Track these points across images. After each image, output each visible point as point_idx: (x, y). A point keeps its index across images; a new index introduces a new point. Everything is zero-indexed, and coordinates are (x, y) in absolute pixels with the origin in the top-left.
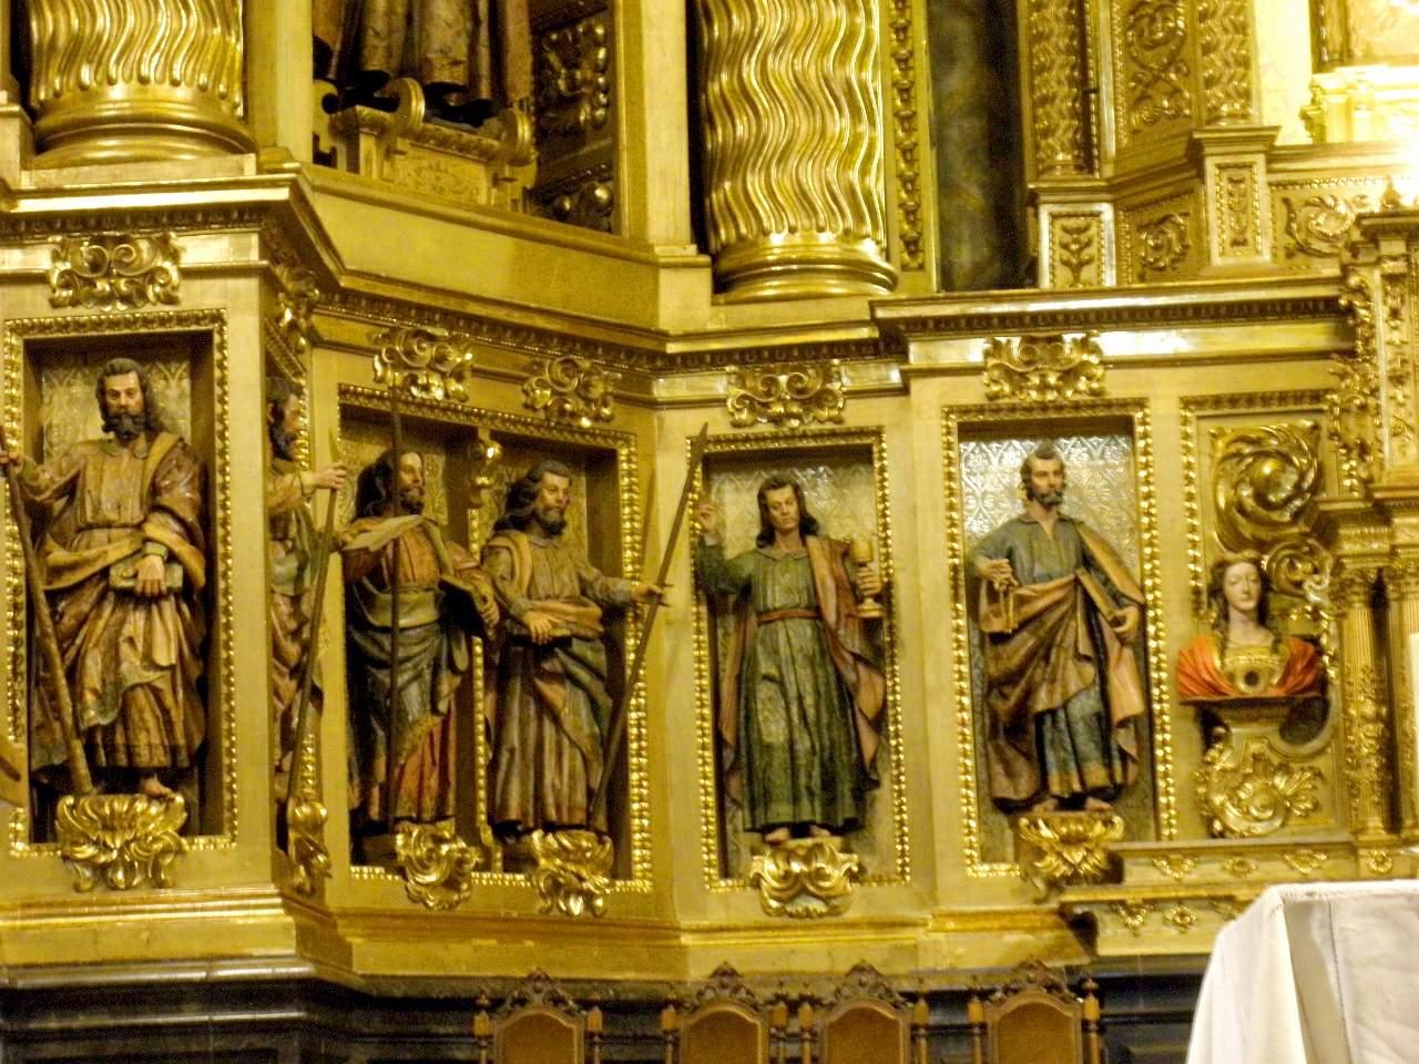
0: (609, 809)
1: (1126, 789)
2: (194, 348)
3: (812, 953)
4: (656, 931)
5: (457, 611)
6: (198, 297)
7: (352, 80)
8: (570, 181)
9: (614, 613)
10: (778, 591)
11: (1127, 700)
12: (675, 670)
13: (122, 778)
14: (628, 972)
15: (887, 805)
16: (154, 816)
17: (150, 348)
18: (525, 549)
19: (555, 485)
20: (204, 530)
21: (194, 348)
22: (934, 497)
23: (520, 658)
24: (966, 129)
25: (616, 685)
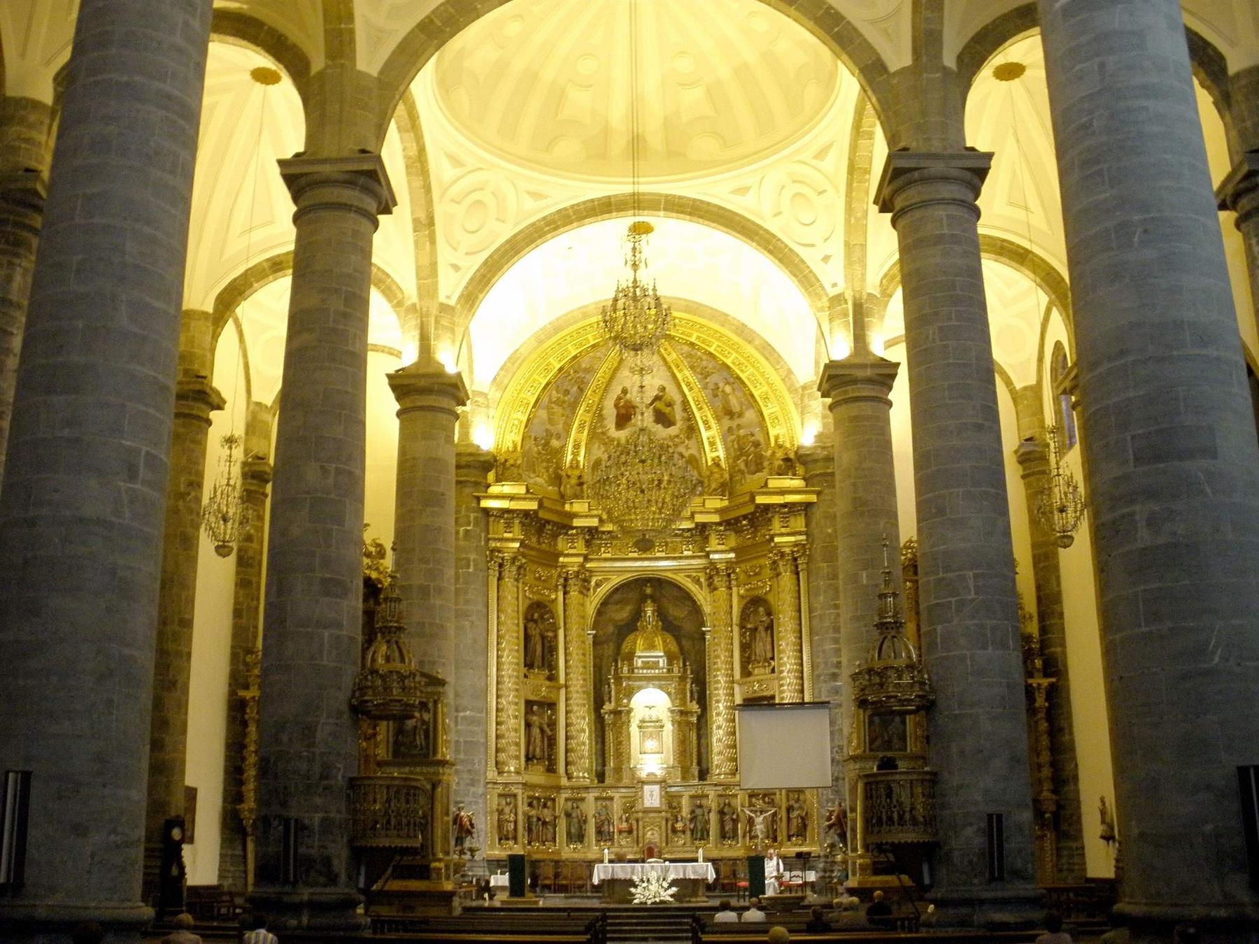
1: (612, 839)
2: (515, 796)
3: (576, 856)
4: (558, 852)
5: (539, 819)
7: (529, 758)
8: (551, 769)
12: (562, 825)
13: (507, 839)
14: (556, 858)
15: (586, 839)
17: (510, 796)
18: (546, 811)
19: (549, 803)
20: (516, 815)
21: (515, 796)
22: (590, 807)
23: (545, 823)
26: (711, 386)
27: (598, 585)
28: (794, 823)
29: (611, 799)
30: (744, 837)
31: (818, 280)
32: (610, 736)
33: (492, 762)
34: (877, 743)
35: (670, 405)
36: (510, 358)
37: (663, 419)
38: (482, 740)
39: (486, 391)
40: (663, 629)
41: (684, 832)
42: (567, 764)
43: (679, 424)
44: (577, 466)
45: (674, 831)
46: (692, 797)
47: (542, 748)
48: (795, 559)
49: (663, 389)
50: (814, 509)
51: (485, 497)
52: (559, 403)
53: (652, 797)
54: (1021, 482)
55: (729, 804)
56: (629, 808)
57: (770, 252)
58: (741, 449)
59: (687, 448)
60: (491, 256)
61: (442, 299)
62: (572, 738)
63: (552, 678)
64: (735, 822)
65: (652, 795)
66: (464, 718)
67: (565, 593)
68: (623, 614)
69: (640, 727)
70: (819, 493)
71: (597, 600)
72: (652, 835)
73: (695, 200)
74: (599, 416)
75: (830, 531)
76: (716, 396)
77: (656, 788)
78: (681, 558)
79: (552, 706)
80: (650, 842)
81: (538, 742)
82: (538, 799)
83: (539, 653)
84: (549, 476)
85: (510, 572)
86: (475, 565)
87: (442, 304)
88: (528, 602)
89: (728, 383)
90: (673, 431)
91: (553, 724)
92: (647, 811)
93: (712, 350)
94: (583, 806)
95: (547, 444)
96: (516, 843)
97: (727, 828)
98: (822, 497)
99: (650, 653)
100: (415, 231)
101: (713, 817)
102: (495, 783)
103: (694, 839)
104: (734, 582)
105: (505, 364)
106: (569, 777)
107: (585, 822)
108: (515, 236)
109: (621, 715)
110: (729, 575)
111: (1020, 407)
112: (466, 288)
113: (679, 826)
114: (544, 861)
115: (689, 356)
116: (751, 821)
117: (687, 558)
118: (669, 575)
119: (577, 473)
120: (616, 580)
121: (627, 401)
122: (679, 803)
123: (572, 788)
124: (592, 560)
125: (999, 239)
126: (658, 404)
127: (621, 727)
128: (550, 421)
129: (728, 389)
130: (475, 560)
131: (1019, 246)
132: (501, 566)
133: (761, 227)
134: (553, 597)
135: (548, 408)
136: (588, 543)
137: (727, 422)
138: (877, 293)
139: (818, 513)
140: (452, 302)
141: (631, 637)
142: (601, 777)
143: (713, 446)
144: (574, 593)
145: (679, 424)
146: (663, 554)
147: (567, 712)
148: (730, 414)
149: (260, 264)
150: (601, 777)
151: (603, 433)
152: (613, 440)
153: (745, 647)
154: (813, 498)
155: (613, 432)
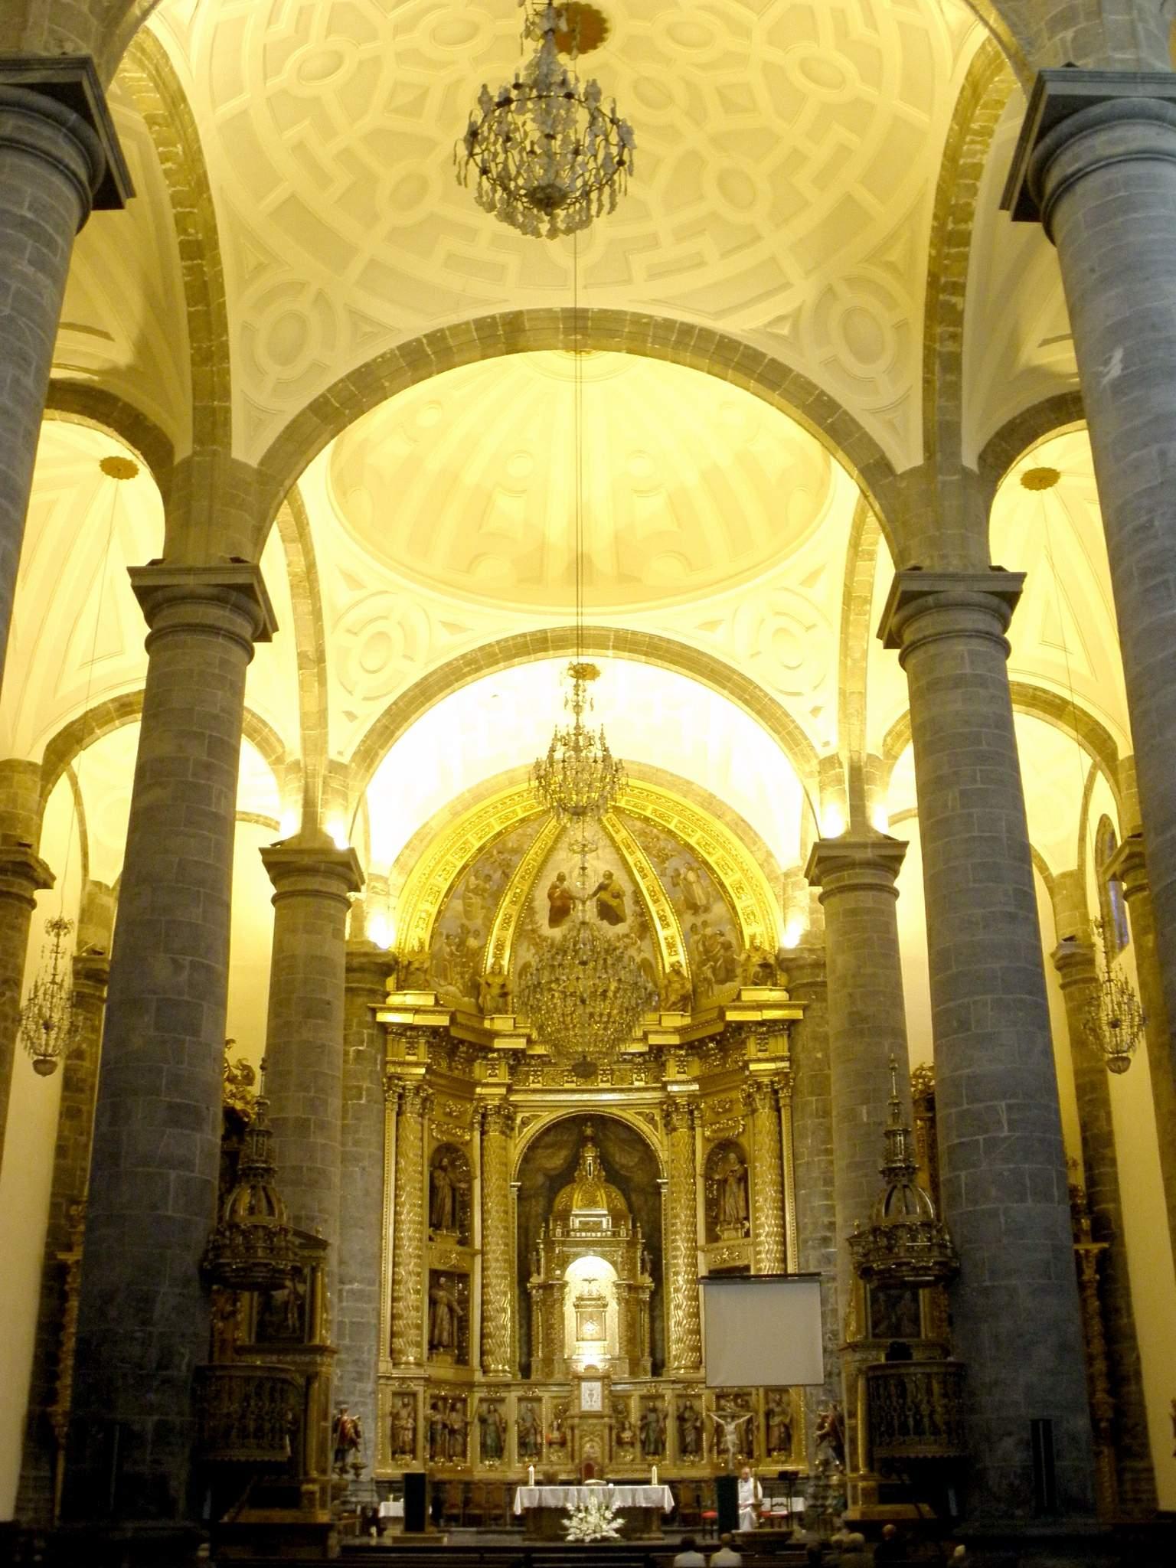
0: (464, 1454)
1: (539, 1454)
2: (414, 1395)
3: (493, 1476)
5: (445, 1426)
6: (416, 1388)
7: (433, 1346)
8: (462, 1360)
9: (467, 1424)
10: (490, 1421)
11: (539, 1440)
13: (403, 1452)
14: (466, 1478)
15: (506, 1453)
16: (408, 1457)
18: (454, 1414)
19: (459, 1405)
20: (415, 1420)
21: (414, 1395)
22: (511, 1410)
23: (452, 1432)
24: (524, 1339)
25: (466, 1435)
26: (670, 872)
27: (524, 1123)
28: (776, 1433)
29: (539, 1400)
30: (710, 1451)
31: (806, 738)
32: (538, 1318)
33: (385, 1350)
34: (882, 1327)
35: (618, 896)
36: (417, 834)
37: (609, 913)
38: (374, 1321)
39: (385, 874)
40: (606, 1181)
41: (632, 1444)
42: (483, 1353)
43: (630, 920)
44: (500, 973)
45: (620, 1442)
46: (643, 1398)
47: (451, 1332)
48: (776, 1092)
49: (609, 876)
50: (800, 1028)
51: (382, 1009)
52: (476, 891)
53: (591, 1398)
54: (1061, 992)
55: (691, 1408)
56: (562, 1412)
57: (746, 702)
58: (707, 951)
59: (640, 950)
60: (395, 703)
61: (333, 755)
62: (490, 1319)
63: (464, 1242)
64: (699, 1431)
65: (591, 1395)
66: (352, 1291)
67: (483, 1133)
68: (556, 1161)
69: (577, 1306)
70: (805, 1008)
71: (524, 1141)
72: (592, 1448)
73: (652, 637)
74: (529, 909)
75: (819, 1055)
76: (675, 885)
77: (598, 1385)
78: (630, 1090)
79: (464, 1277)
80: (589, 1458)
81: (446, 1325)
82: (445, 1399)
83: (448, 1210)
84: (464, 984)
85: (413, 1104)
86: (368, 1095)
87: (331, 762)
88: (435, 1144)
89: (691, 869)
90: (621, 928)
91: (465, 1301)
92: (585, 1416)
93: (671, 827)
94: (502, 1409)
95: (462, 944)
96: (414, 1458)
97: (688, 1439)
98: (808, 1013)
99: (591, 1210)
100: (300, 668)
101: (671, 1425)
102: (389, 1378)
103: (645, 1453)
104: (697, 1122)
105: (410, 842)
106: (485, 1371)
107: (505, 1430)
108: (425, 678)
109: (553, 1290)
110: (691, 1112)
111: (1057, 899)
112: (363, 742)
113: (627, 1435)
114: (450, 1482)
115: (643, 834)
116: (719, 1430)
117: (638, 1090)
118: (615, 1111)
119: (499, 980)
120: (547, 1118)
121: (564, 891)
122: (627, 1406)
123: (489, 1385)
124: (517, 1091)
125: (1029, 686)
126: (603, 895)
127: (553, 1306)
128: (467, 914)
129: (691, 876)
130: (368, 1089)
131: (1055, 696)
132: (401, 1097)
133: (734, 671)
134: (467, 1138)
135: (464, 898)
136: (513, 1071)
137: (689, 919)
138: (879, 752)
139: (804, 1033)
140: (345, 760)
141: (568, 1189)
142: (526, 1370)
143: (672, 948)
144: (494, 1134)
145: (630, 920)
146: (607, 1085)
147: (483, 1287)
148: (694, 908)
149: (105, 704)
150: (526, 1370)
151: (533, 931)
152: (545, 939)
153: (711, 1204)
154: (798, 1014)
155: (546, 930)
